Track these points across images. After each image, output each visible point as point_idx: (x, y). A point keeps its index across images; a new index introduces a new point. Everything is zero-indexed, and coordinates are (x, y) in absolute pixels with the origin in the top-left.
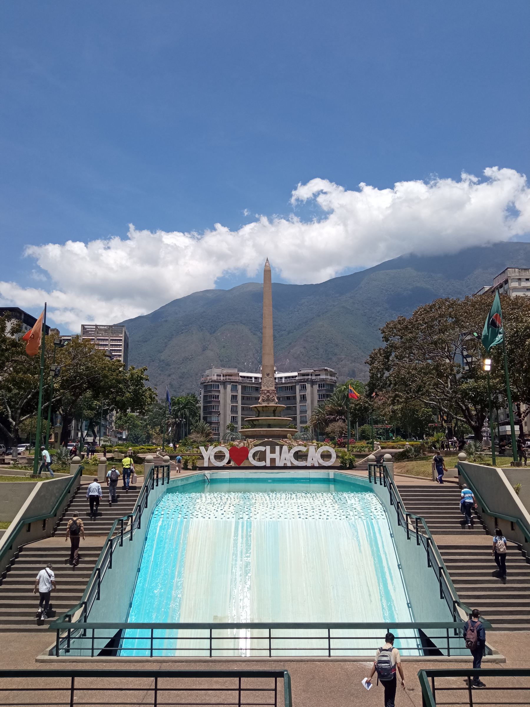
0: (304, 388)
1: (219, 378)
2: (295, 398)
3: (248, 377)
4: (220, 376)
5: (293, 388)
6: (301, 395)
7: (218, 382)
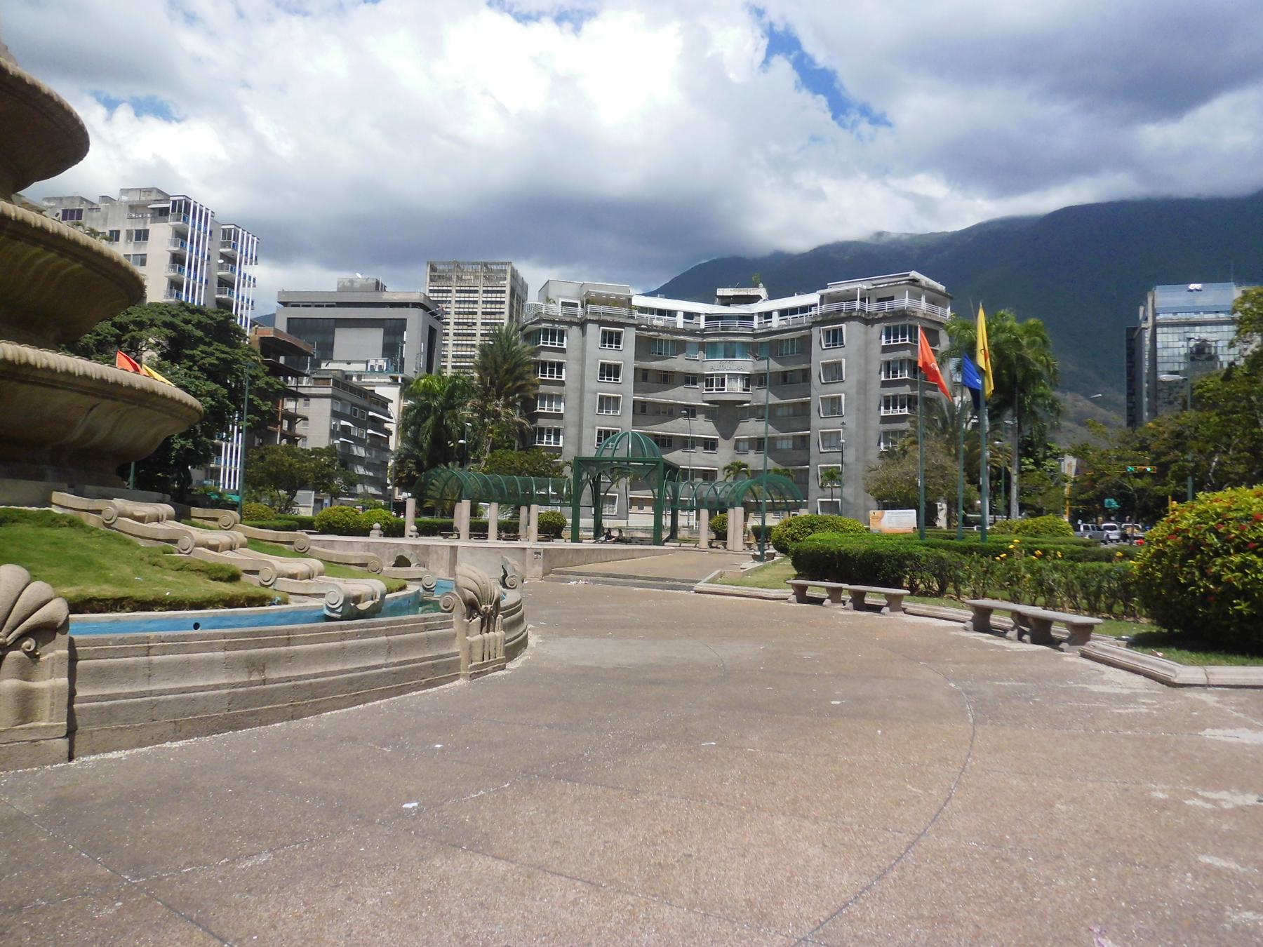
0: (835, 338)
1: (570, 310)
2: (806, 374)
3: (661, 312)
4: (575, 305)
5: (803, 346)
6: (826, 366)
7: (561, 322)
